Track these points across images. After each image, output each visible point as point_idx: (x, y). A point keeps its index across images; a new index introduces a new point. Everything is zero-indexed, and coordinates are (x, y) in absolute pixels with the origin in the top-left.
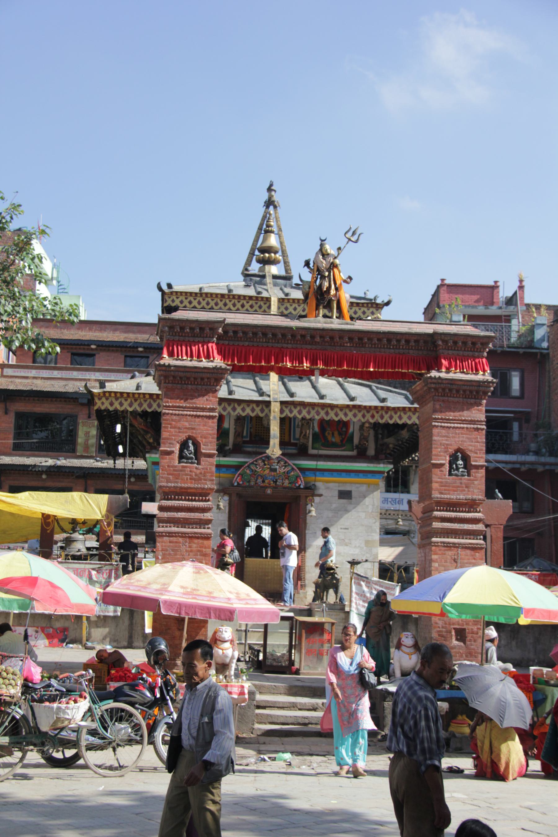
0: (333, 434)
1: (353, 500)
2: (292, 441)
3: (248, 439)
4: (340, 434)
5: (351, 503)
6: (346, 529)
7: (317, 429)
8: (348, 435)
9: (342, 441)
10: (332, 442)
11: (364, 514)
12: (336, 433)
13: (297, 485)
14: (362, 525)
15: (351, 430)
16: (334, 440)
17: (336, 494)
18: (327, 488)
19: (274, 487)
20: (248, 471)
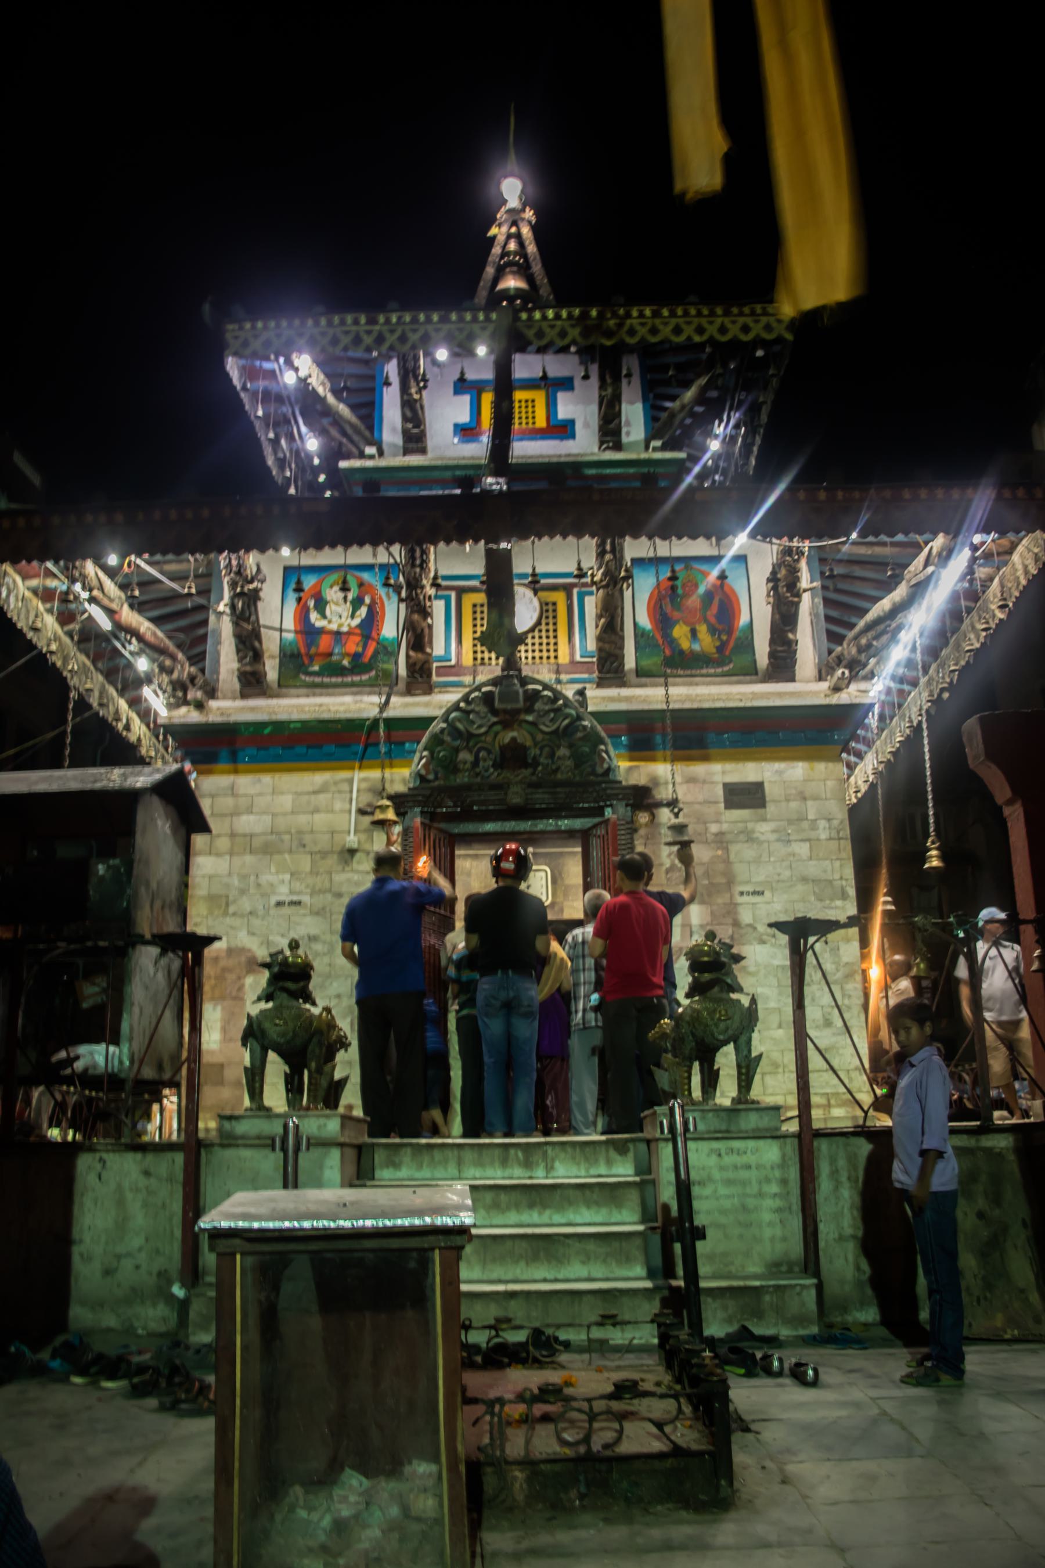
0: (694, 633)
1: (771, 809)
2: (578, 658)
3: (453, 662)
4: (712, 631)
5: (764, 820)
6: (756, 893)
7: (645, 621)
8: (737, 634)
9: (720, 649)
10: (692, 652)
11: (807, 845)
12: (702, 629)
13: (600, 771)
14: (804, 880)
15: (744, 619)
16: (696, 647)
17: (720, 792)
18: (691, 780)
19: (531, 785)
20: (447, 738)
